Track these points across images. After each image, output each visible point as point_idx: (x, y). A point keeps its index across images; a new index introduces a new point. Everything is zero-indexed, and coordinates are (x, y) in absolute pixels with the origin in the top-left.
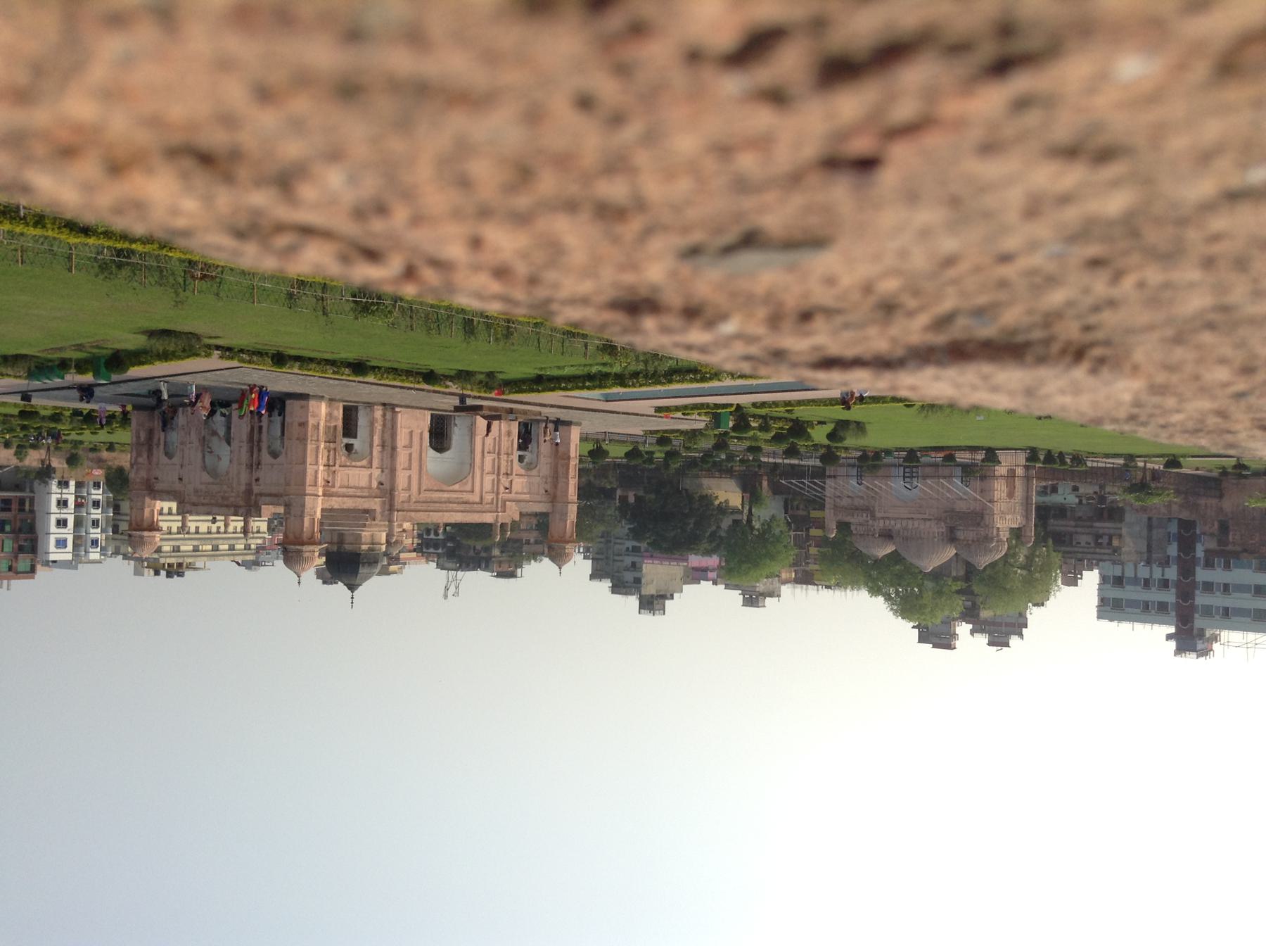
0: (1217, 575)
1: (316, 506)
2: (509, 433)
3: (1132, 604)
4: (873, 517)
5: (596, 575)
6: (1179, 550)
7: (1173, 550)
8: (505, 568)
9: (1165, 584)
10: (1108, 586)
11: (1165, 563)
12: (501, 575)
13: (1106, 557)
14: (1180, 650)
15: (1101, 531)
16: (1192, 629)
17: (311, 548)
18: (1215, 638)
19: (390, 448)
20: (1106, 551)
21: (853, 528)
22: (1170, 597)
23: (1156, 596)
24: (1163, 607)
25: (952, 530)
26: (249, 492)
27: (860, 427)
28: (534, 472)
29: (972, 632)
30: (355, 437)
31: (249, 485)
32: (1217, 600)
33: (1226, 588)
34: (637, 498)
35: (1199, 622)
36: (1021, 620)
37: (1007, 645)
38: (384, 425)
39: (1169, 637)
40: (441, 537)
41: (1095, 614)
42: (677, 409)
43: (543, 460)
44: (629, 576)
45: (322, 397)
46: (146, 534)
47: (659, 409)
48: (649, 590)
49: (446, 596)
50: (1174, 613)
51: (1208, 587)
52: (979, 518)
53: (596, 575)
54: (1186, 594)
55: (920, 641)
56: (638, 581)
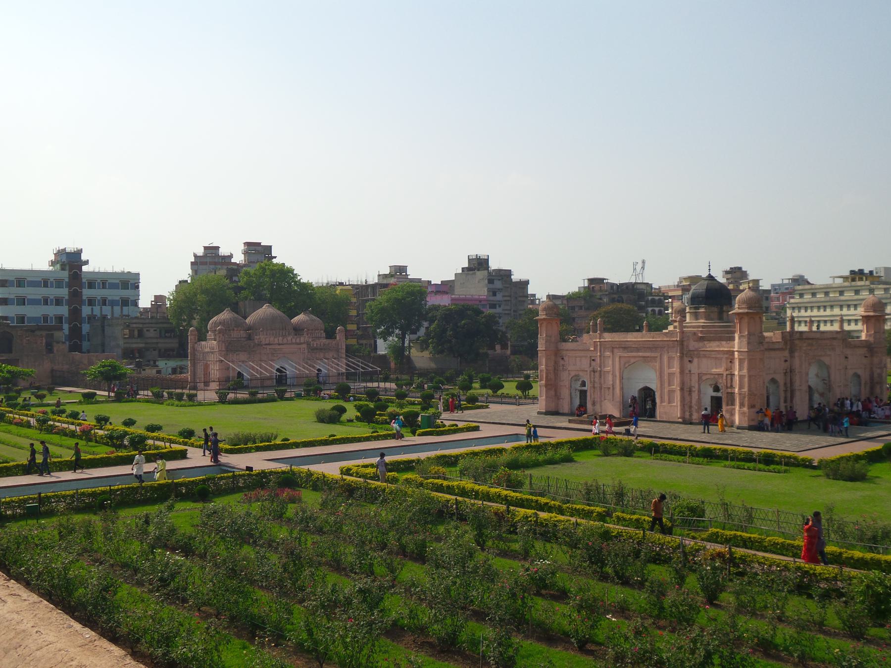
0: (52, 311)
1: (738, 344)
2: (594, 404)
3: (114, 286)
4: (308, 344)
6: (81, 328)
7: (86, 328)
8: (597, 287)
9: (91, 302)
10: (132, 298)
11: (91, 318)
12: (601, 281)
13: (135, 321)
14: (79, 253)
15: (139, 340)
16: (70, 271)
17: (741, 311)
18: (53, 263)
19: (686, 390)
20: (134, 325)
21: (324, 335)
22: (87, 293)
23: (97, 293)
24: (91, 285)
25: (249, 338)
26: (792, 352)
27: (324, 418)
28: (573, 374)
29: (231, 256)
30: (712, 397)
31: (792, 357)
32: (52, 292)
33: (46, 301)
34: (493, 348)
35: (65, 275)
36: (196, 267)
37: (206, 248)
38: (691, 407)
39: (87, 263)
40: (650, 309)
41: (141, 277)
42: (462, 430)
43: (567, 383)
44: (498, 284)
45: (738, 428)
46: (872, 314)
47: (476, 429)
48: (481, 274)
49: (644, 262)
50: (84, 280)
51: (58, 302)
52: (230, 348)
54: (75, 296)
55: (271, 247)
56: (491, 281)
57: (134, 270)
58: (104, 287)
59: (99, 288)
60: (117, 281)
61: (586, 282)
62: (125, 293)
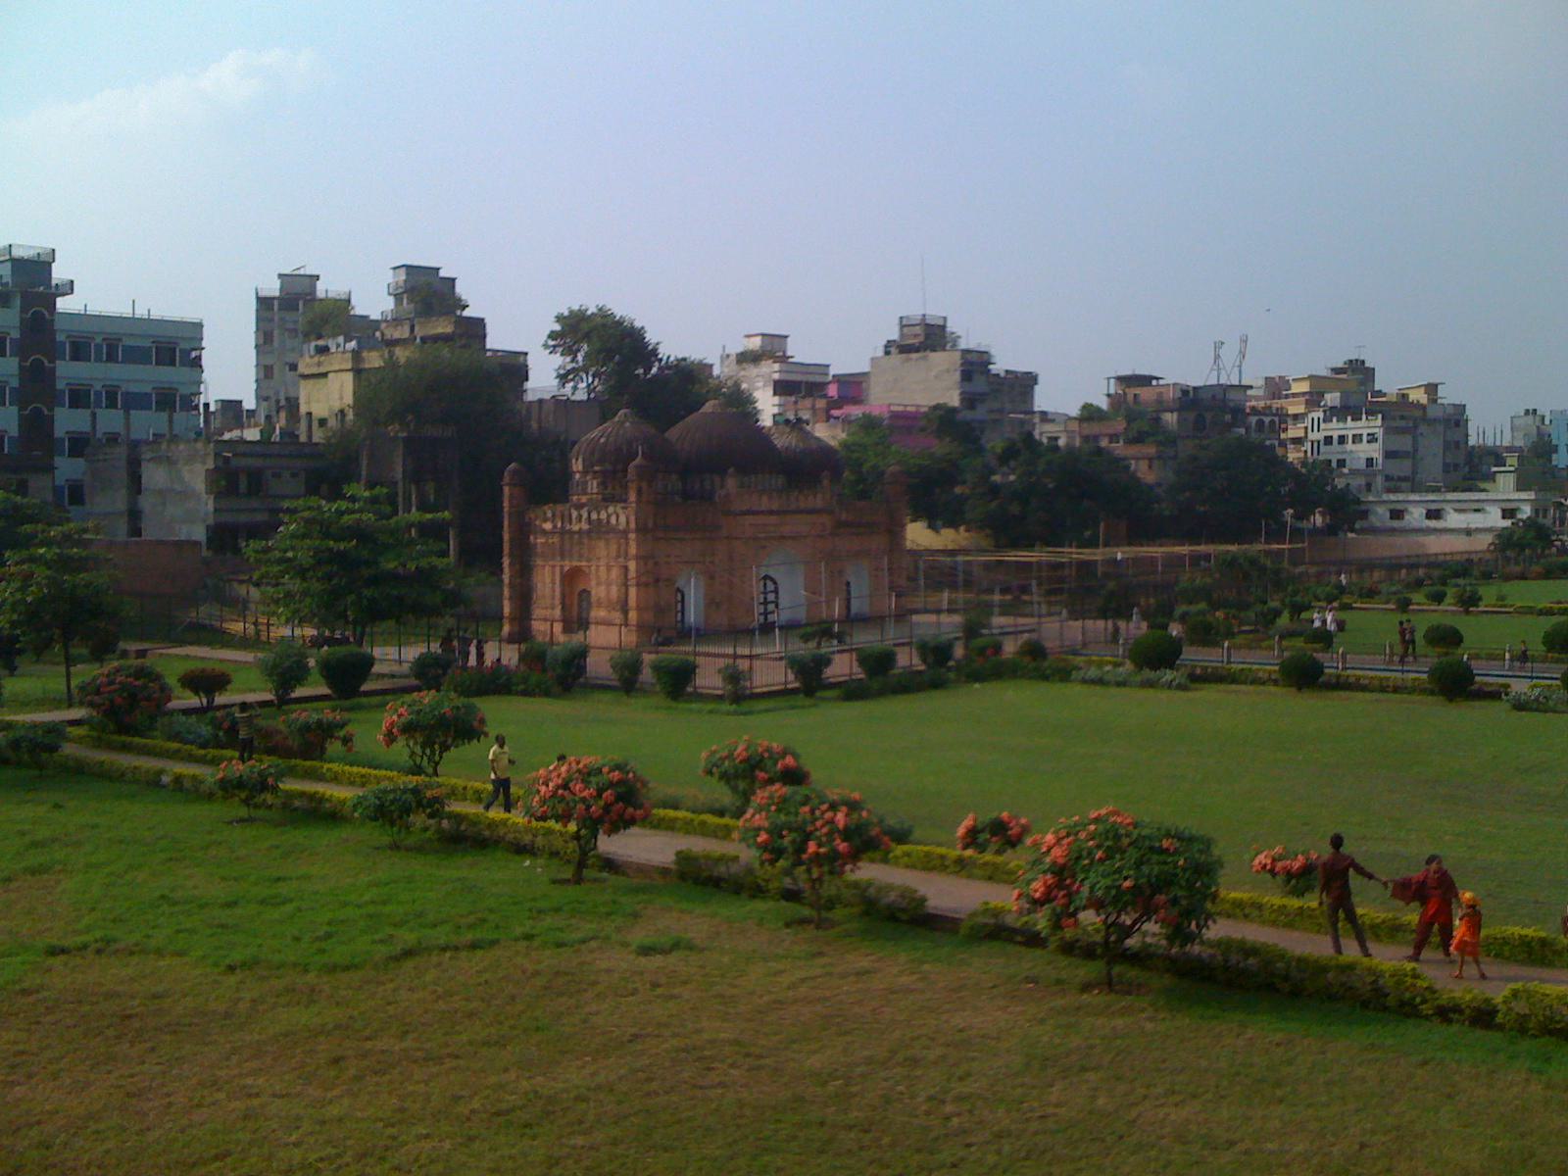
3: (137, 355)
5: (1023, 384)
9: (79, 398)
10: (184, 390)
12: (1145, 381)
16: (23, 310)
22: (68, 371)
24: (80, 350)
39: (69, 288)
41: (206, 332)
49: (1244, 341)
50: (60, 337)
53: (1023, 384)
57: (187, 314)
58: (111, 357)
59: (98, 359)
60: (147, 343)
61: (1112, 381)
62: (166, 375)
